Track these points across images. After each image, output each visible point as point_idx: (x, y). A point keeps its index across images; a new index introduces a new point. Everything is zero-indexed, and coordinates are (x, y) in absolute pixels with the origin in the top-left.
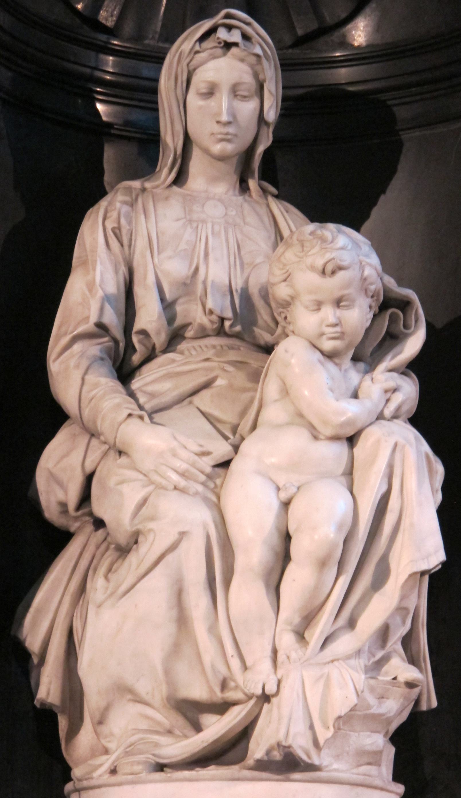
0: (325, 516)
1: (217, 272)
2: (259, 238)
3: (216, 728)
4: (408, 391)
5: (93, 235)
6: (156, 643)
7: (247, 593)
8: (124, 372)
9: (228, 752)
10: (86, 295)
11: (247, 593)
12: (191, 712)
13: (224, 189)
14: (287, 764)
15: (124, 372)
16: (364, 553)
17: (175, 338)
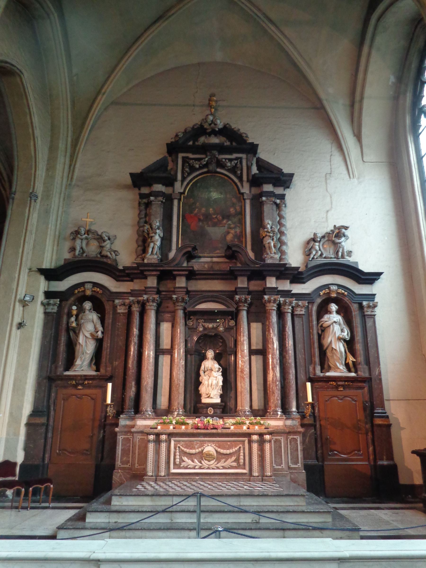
0: (214, 382)
1: (210, 366)
2: (213, 363)
3: (209, 395)
4: (221, 374)
5: (203, 364)
6: (205, 390)
7: (210, 387)
8: (204, 372)
9: (208, 397)
10: (202, 367)
11: (210, 387)
12: (207, 394)
13: (211, 360)
14: (212, 398)
15: (204, 372)
16: (217, 384)
17: (207, 370)
